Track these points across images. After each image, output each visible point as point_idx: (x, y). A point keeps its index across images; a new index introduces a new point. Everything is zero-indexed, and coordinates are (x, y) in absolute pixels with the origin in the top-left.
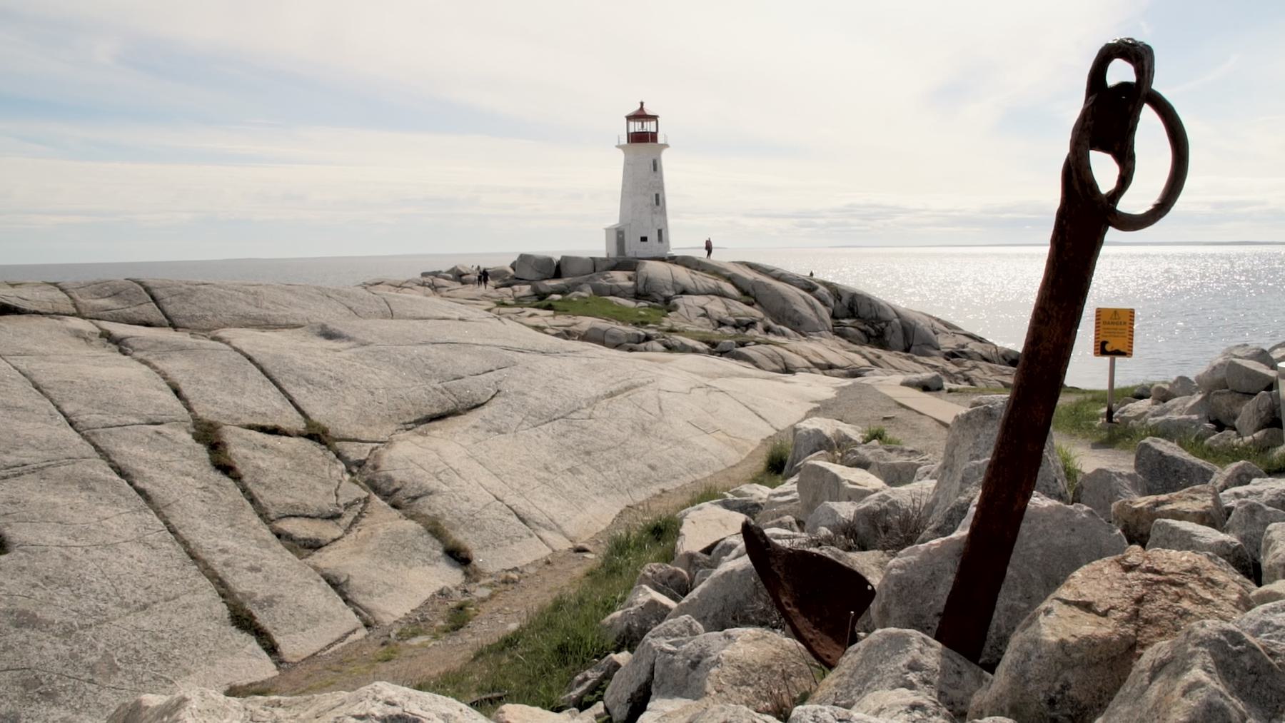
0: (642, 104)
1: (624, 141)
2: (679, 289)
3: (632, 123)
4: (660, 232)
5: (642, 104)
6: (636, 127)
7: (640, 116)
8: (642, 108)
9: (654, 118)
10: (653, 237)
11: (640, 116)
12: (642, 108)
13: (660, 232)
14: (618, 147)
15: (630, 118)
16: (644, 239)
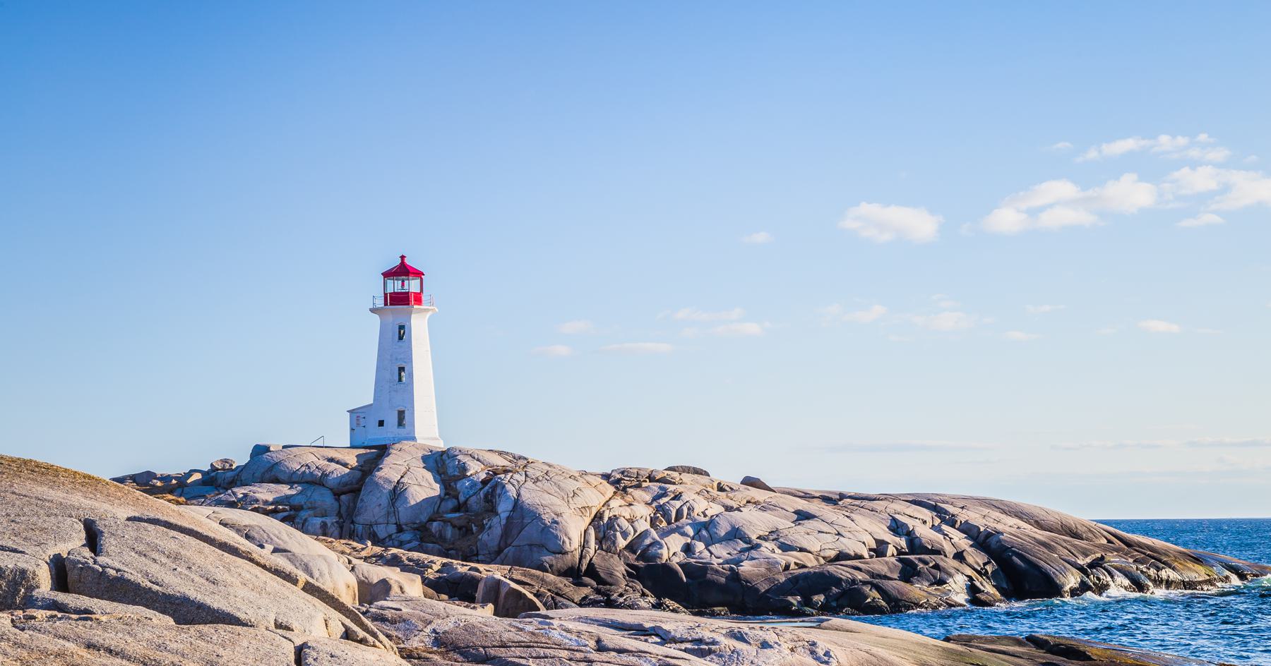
0: (403, 257)
1: (380, 303)
2: (267, 476)
3: (390, 282)
4: (401, 414)
5: (403, 257)
6: (395, 286)
7: (403, 270)
8: (403, 262)
9: (419, 274)
10: (392, 419)
11: (403, 270)
12: (403, 262)
13: (401, 414)
14: (373, 310)
15: (387, 275)
16: (381, 423)
